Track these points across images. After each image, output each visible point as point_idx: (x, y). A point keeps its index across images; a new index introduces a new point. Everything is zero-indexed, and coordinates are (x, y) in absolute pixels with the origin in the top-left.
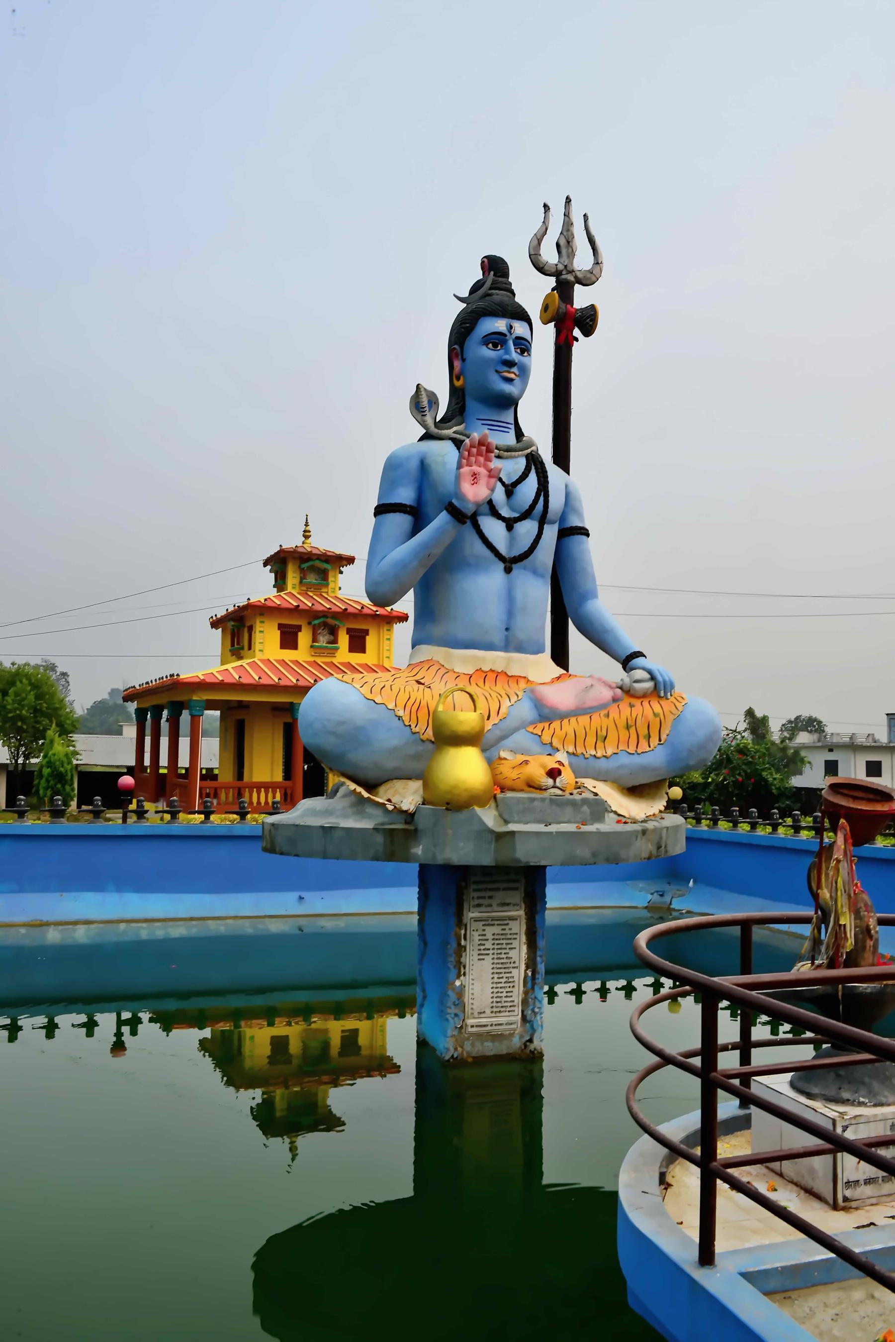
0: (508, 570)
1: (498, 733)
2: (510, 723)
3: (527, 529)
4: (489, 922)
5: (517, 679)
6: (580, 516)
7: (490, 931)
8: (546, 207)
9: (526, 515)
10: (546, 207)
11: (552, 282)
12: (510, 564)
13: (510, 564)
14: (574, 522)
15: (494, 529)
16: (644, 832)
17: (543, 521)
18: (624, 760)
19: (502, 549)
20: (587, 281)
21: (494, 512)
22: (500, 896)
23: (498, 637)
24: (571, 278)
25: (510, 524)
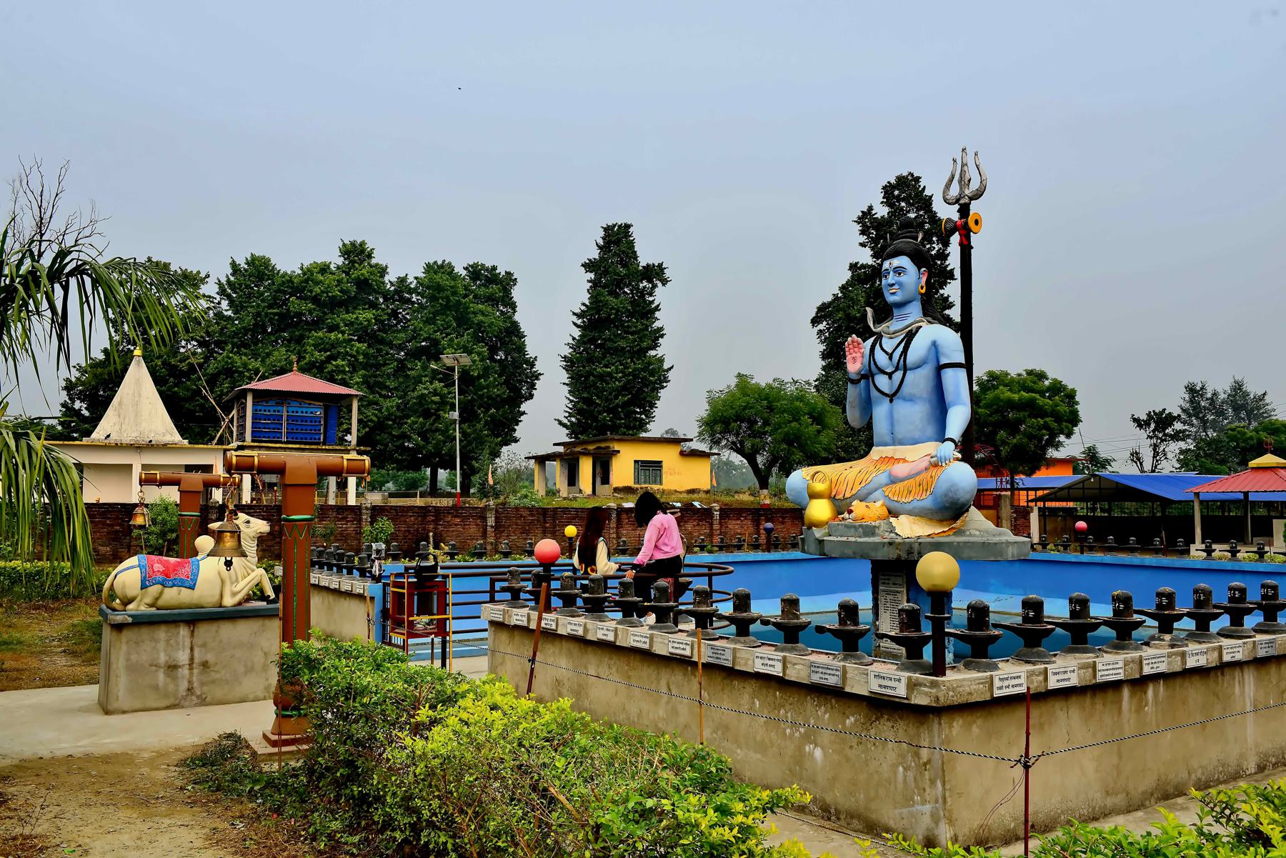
0: (891, 401)
1: (865, 491)
2: (872, 486)
3: (899, 375)
4: (888, 593)
5: (899, 460)
6: (947, 356)
7: (889, 597)
8: (955, 161)
9: (897, 369)
10: (955, 161)
11: (957, 207)
12: (892, 397)
13: (892, 397)
14: (944, 361)
15: (882, 381)
16: (890, 544)
17: (905, 370)
18: (915, 504)
19: (886, 391)
20: (978, 195)
21: (883, 372)
22: (893, 579)
23: (888, 438)
24: (967, 200)
25: (890, 375)
